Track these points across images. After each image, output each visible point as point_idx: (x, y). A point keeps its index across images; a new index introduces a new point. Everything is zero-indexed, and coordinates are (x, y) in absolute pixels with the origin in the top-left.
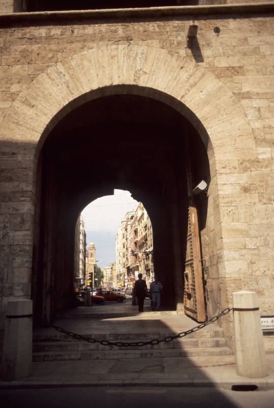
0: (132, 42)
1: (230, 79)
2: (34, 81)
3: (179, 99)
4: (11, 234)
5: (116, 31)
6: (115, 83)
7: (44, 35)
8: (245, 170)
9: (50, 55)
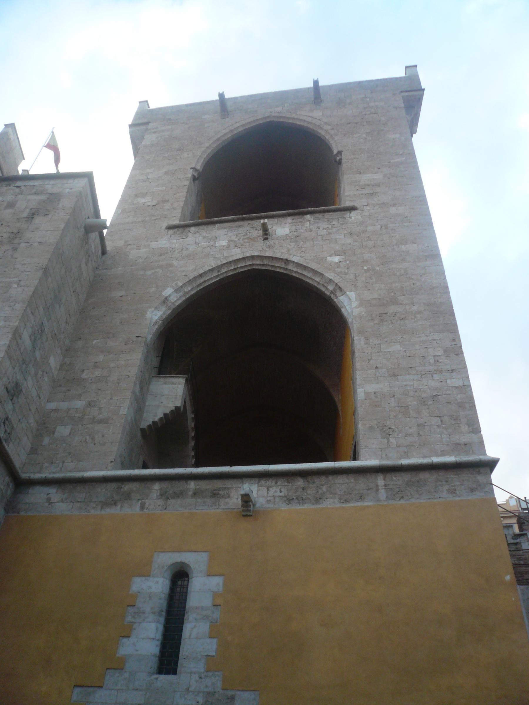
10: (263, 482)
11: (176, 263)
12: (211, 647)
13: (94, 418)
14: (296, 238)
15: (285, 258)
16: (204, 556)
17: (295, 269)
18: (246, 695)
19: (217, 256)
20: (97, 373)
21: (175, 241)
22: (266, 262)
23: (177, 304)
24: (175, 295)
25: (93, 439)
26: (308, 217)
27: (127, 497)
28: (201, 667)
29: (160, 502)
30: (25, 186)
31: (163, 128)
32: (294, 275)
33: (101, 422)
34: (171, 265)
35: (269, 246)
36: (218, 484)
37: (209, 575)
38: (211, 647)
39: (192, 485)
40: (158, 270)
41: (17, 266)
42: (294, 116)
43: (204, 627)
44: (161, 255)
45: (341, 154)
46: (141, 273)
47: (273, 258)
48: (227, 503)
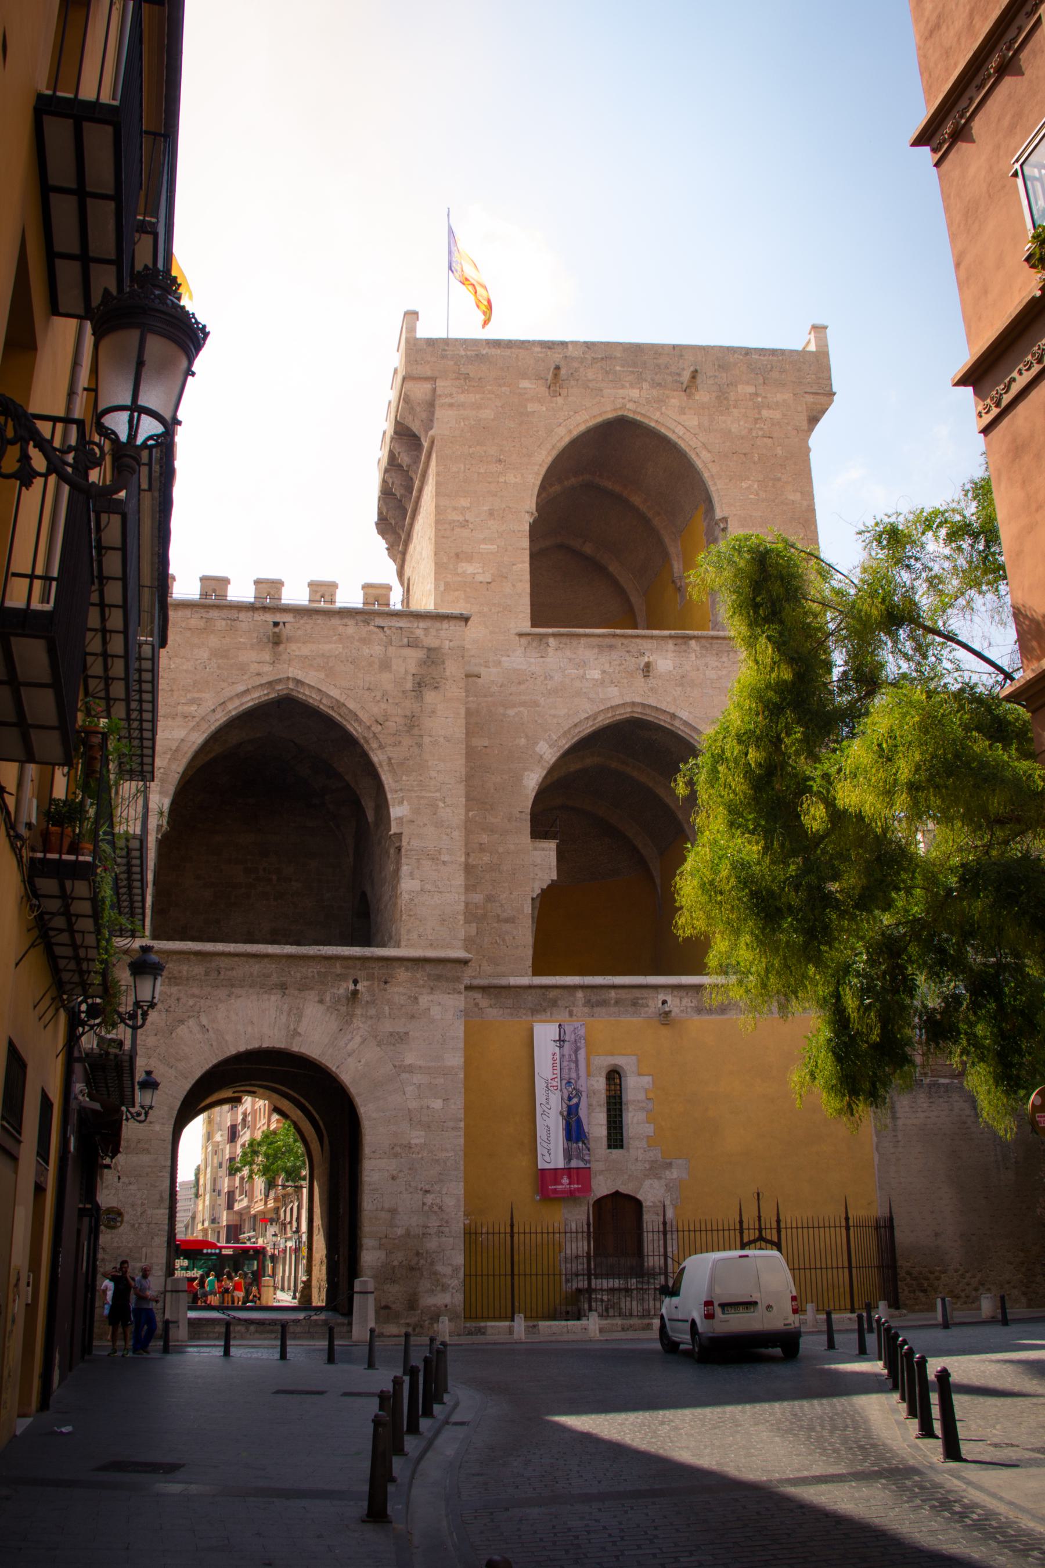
0: (287, 992)
1: (392, 1048)
2: (174, 1035)
3: (334, 1069)
4: (149, 1212)
5: (269, 976)
6: (265, 1046)
7: (185, 973)
8: (396, 1155)
9: (191, 1002)
10: (675, 993)
11: (542, 701)
12: (649, 1129)
13: (498, 916)
14: (682, 681)
15: (672, 711)
16: (633, 1059)
17: (682, 728)
18: (680, 1161)
19: (591, 696)
20: (486, 858)
21: (532, 660)
22: (648, 711)
23: (551, 762)
24: (550, 751)
25: (504, 940)
26: (693, 643)
27: (554, 1003)
28: (644, 1144)
29: (586, 1010)
30: (390, 628)
31: (462, 398)
32: (680, 733)
33: (507, 921)
34: (536, 704)
35: (652, 689)
36: (637, 993)
37: (639, 1075)
38: (649, 1129)
39: (613, 993)
40: (522, 709)
41: (433, 774)
42: (657, 416)
43: (642, 1116)
44: (519, 683)
45: (727, 522)
46: (501, 710)
47: (657, 709)
48: (646, 1012)
